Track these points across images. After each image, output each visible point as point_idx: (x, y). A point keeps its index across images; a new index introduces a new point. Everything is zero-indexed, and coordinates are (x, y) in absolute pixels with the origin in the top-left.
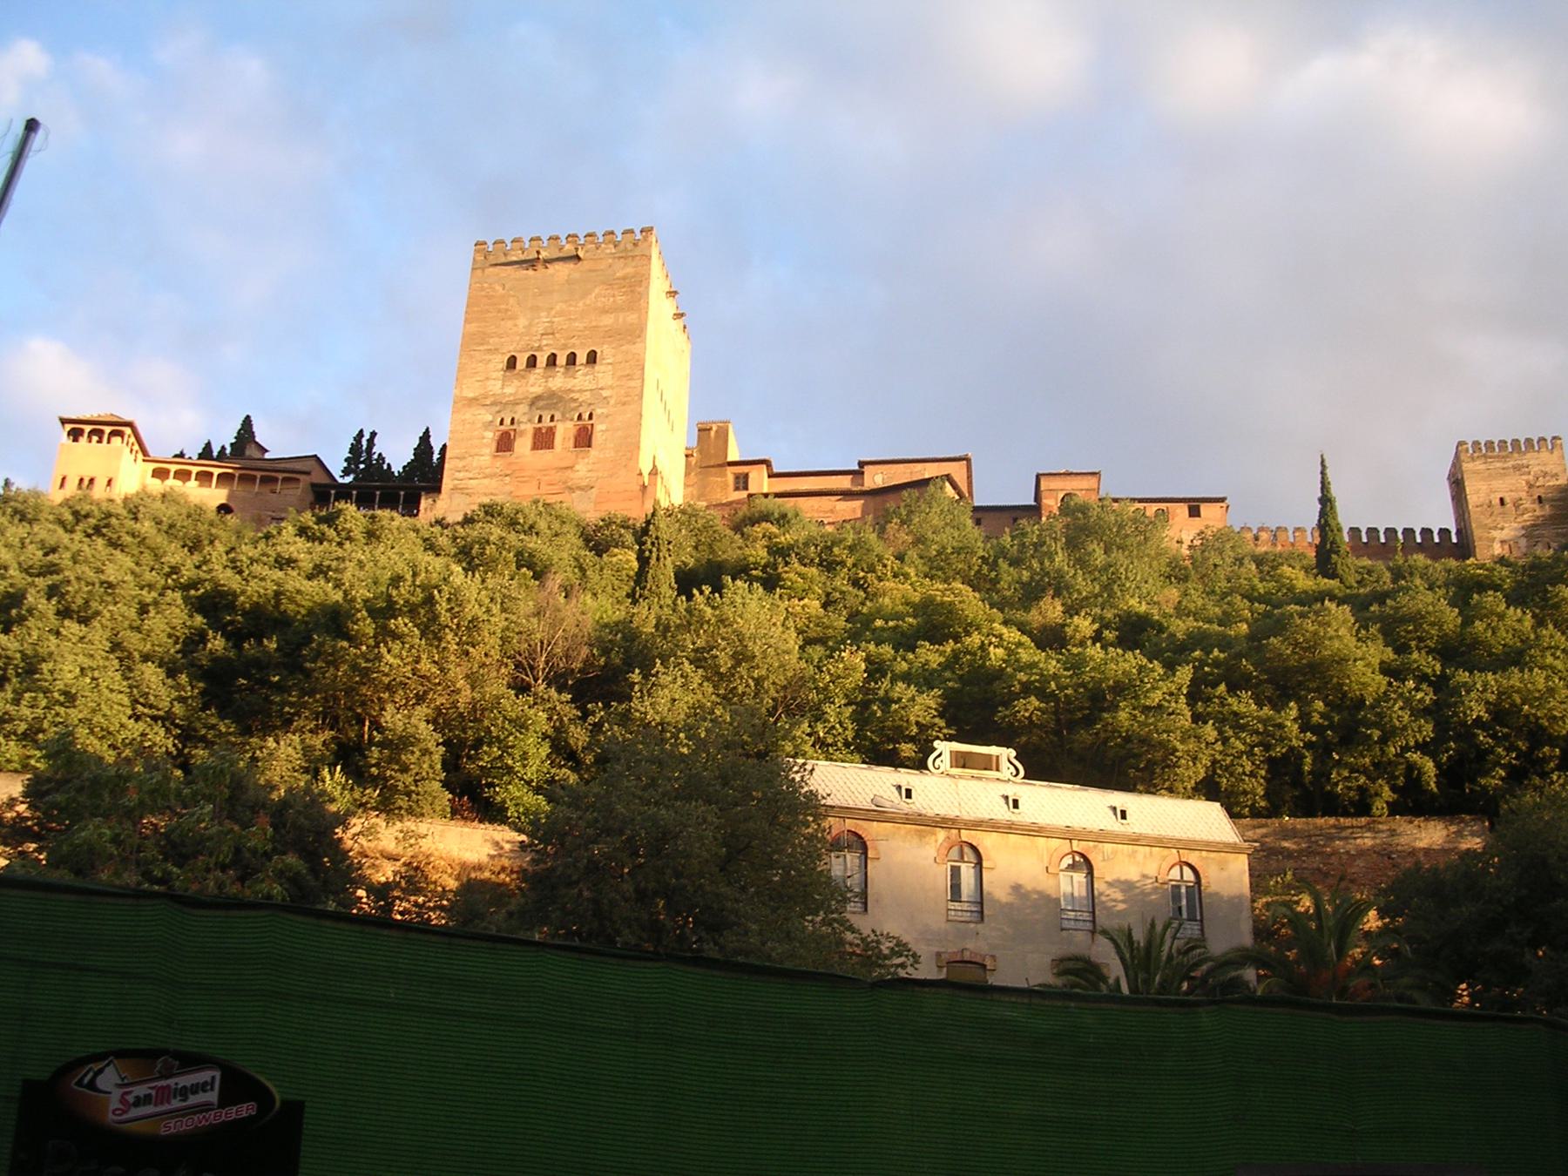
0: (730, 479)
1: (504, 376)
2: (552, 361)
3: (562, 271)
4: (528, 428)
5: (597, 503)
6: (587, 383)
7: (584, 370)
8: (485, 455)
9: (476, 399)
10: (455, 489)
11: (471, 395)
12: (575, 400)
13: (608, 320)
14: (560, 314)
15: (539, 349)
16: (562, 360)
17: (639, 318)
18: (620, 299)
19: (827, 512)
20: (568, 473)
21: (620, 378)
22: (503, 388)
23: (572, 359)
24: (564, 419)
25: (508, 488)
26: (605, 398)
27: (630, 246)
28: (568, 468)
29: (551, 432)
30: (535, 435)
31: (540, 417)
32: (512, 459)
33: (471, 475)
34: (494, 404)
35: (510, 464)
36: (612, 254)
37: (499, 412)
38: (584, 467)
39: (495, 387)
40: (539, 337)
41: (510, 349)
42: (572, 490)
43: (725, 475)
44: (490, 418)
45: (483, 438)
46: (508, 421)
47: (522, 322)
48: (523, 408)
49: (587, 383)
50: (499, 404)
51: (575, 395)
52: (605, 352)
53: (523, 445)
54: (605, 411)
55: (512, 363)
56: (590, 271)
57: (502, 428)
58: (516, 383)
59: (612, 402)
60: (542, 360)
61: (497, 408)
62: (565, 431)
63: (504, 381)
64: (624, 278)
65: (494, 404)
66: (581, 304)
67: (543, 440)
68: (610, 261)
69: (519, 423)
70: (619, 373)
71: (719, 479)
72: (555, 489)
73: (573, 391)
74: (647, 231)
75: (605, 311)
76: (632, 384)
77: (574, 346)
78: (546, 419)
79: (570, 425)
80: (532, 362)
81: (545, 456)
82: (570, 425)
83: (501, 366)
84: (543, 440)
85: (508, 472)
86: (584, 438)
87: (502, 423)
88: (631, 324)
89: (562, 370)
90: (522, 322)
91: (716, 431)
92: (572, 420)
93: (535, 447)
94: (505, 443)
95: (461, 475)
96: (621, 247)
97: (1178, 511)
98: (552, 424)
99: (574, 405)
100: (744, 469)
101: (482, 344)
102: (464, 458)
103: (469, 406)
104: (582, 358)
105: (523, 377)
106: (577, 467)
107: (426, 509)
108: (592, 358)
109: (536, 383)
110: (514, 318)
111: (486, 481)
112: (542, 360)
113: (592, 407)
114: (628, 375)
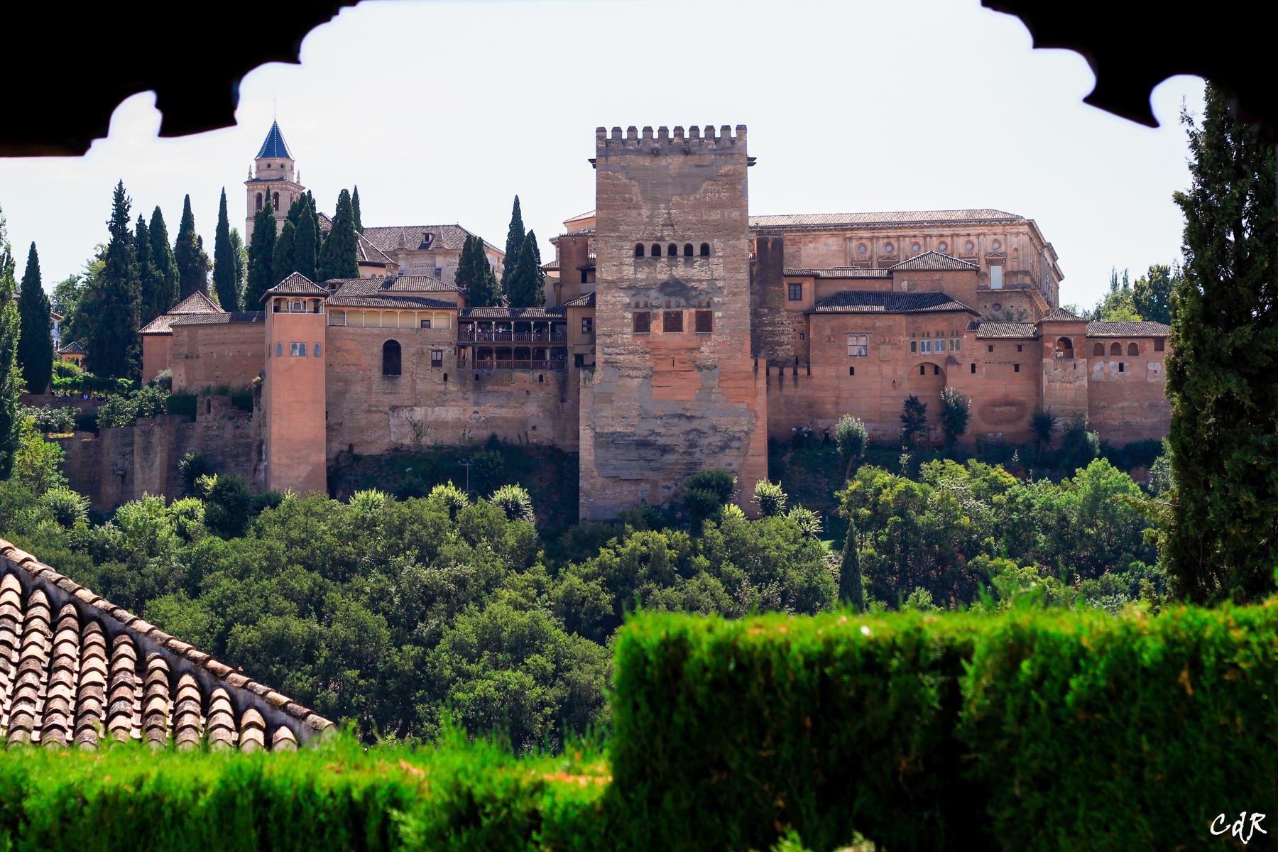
0: (786, 286)
1: (635, 262)
2: (672, 250)
3: (674, 163)
4: (661, 311)
5: (721, 381)
6: (703, 274)
7: (699, 261)
8: (627, 335)
9: (613, 282)
10: (606, 362)
11: (610, 278)
12: (695, 289)
13: (715, 215)
14: (678, 206)
15: (662, 239)
16: (681, 251)
17: (741, 215)
18: (724, 195)
19: (867, 328)
20: (696, 354)
21: (729, 271)
22: (635, 274)
23: (689, 250)
24: (689, 306)
25: (649, 364)
26: (720, 288)
27: (728, 144)
28: (694, 349)
29: (679, 316)
30: (666, 320)
31: (669, 302)
32: (650, 338)
33: (618, 351)
34: (630, 288)
35: (648, 342)
36: (712, 150)
37: (634, 295)
38: (707, 350)
39: (629, 272)
40: (660, 227)
41: (637, 236)
42: (700, 368)
43: (782, 286)
44: (627, 300)
45: (624, 318)
46: (642, 305)
47: (645, 212)
48: (653, 294)
49: (703, 274)
50: (633, 288)
51: (696, 285)
52: (716, 244)
53: (657, 327)
54: (720, 299)
55: (639, 251)
56: (697, 166)
57: (637, 310)
58: (646, 270)
59: (725, 292)
60: (664, 250)
61: (633, 292)
62: (688, 316)
63: (636, 267)
64: (726, 175)
65: (630, 288)
66: (692, 198)
67: (673, 323)
68: (713, 157)
69: (653, 307)
70: (729, 267)
71: (777, 289)
72: (687, 367)
73: (694, 281)
74: (741, 129)
75: (713, 206)
76: (740, 276)
77: (690, 238)
78: (673, 304)
79: (693, 310)
80: (656, 251)
81: (675, 338)
82: (693, 310)
83: (632, 252)
84: (673, 323)
85: (648, 350)
86: (704, 323)
87: (637, 306)
88: (735, 221)
89: (682, 259)
90: (645, 212)
91: (773, 244)
92: (694, 307)
93: (667, 329)
94: (642, 323)
95: (610, 350)
96: (722, 142)
97: (1147, 345)
98: (679, 309)
99: (694, 293)
100: (798, 280)
101: (614, 231)
102: (610, 336)
103: (609, 288)
104: (697, 251)
105: (651, 265)
106: (703, 349)
107: (585, 379)
108: (705, 251)
109: (662, 271)
110: (637, 207)
111: (631, 357)
112: (664, 250)
113: (710, 295)
114: (736, 268)
